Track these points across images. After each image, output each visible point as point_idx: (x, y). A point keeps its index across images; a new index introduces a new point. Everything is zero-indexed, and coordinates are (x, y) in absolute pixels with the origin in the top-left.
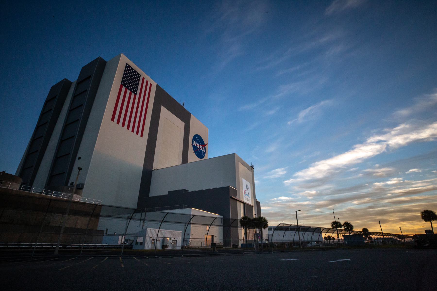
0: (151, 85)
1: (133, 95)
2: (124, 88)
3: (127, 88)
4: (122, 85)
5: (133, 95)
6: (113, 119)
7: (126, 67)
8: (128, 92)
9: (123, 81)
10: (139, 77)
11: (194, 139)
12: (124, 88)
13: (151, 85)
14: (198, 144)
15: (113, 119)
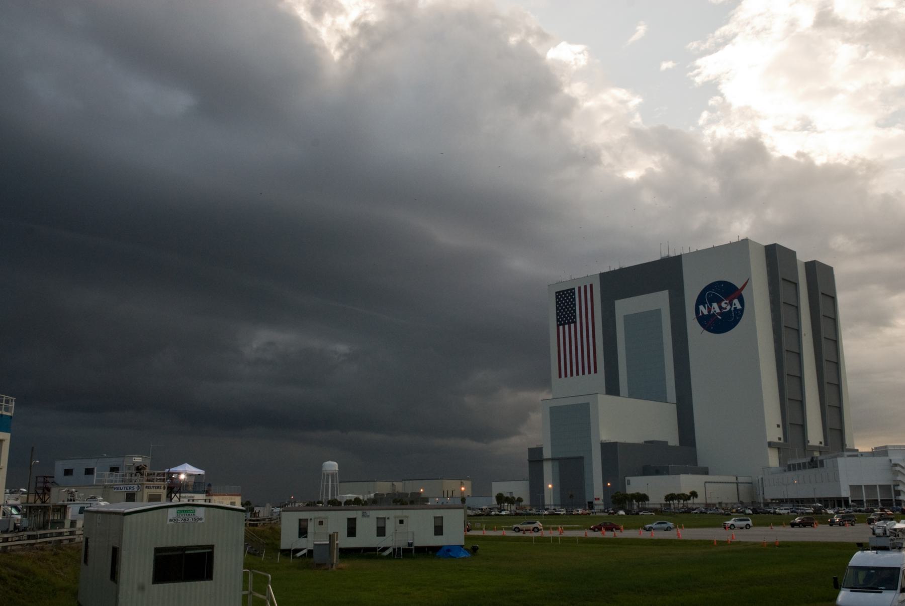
0: (591, 286)
1: (572, 325)
2: (561, 327)
3: (564, 325)
4: (558, 326)
5: (572, 325)
6: (560, 377)
7: (557, 297)
8: (567, 326)
9: (558, 320)
10: (574, 294)
11: (701, 300)
12: (561, 327)
13: (591, 286)
14: (715, 305)
15: (560, 377)
